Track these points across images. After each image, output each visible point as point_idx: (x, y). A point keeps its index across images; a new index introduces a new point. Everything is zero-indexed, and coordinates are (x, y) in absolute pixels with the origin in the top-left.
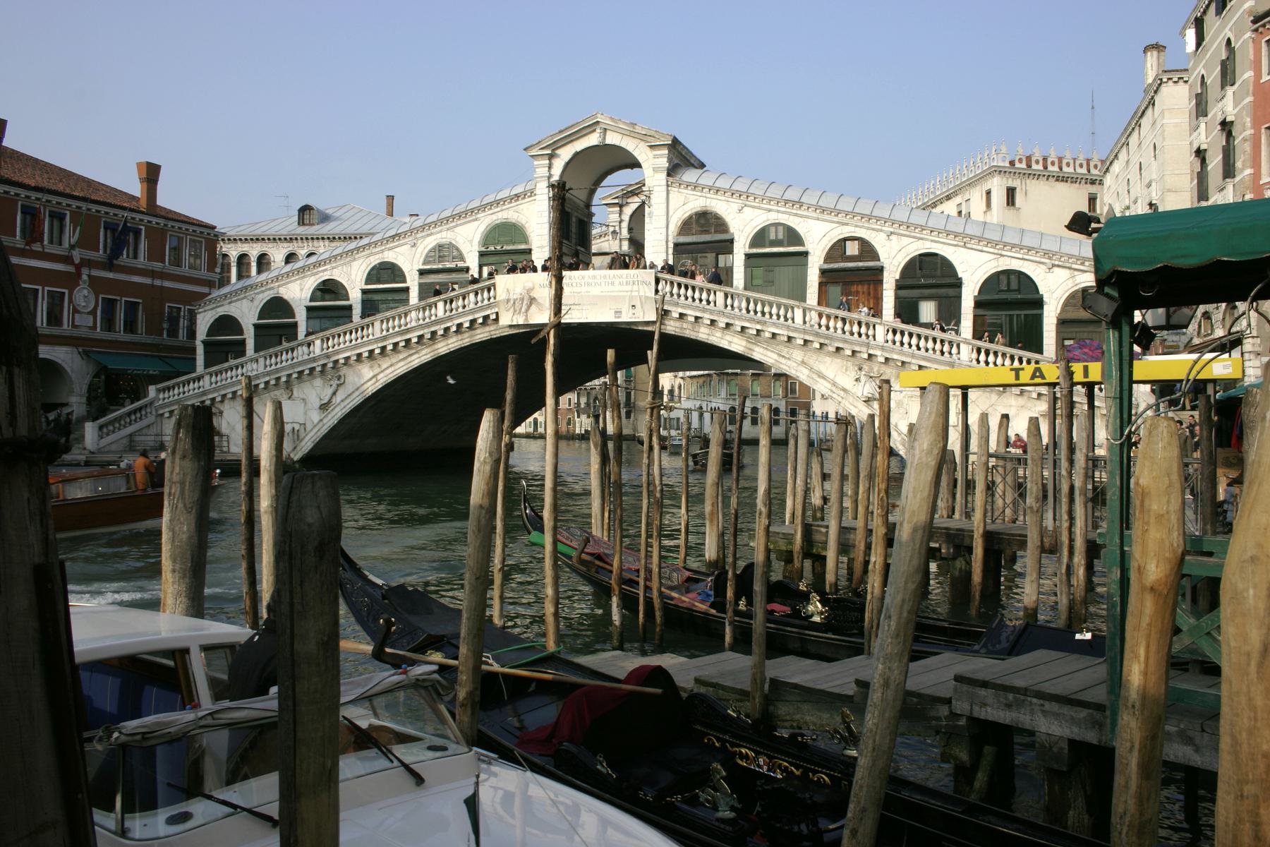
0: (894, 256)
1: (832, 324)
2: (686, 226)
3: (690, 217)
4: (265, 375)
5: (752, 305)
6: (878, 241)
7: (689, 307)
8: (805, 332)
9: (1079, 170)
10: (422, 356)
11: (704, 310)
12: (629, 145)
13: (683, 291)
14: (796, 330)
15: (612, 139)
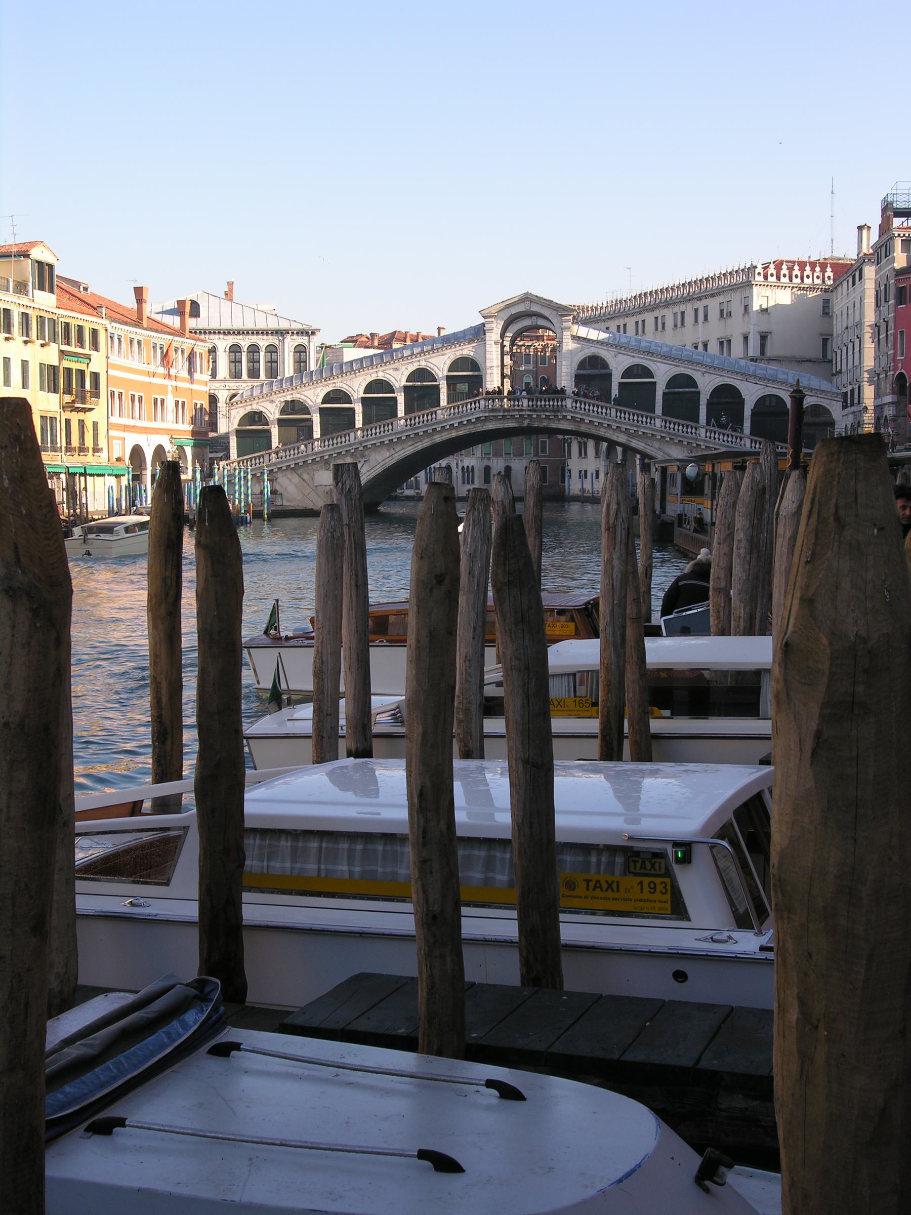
0: (706, 384)
1: (676, 427)
2: (582, 365)
3: (585, 359)
4: (313, 454)
5: (631, 416)
6: (697, 376)
7: (596, 417)
8: (662, 432)
9: (817, 281)
10: (426, 443)
11: (605, 419)
12: (546, 312)
13: (591, 408)
14: (657, 431)
15: (535, 308)
